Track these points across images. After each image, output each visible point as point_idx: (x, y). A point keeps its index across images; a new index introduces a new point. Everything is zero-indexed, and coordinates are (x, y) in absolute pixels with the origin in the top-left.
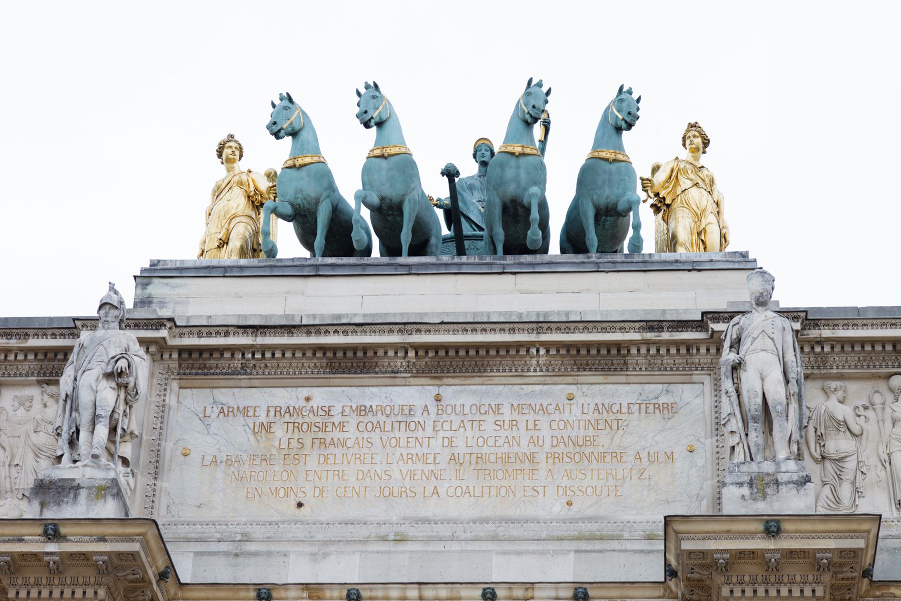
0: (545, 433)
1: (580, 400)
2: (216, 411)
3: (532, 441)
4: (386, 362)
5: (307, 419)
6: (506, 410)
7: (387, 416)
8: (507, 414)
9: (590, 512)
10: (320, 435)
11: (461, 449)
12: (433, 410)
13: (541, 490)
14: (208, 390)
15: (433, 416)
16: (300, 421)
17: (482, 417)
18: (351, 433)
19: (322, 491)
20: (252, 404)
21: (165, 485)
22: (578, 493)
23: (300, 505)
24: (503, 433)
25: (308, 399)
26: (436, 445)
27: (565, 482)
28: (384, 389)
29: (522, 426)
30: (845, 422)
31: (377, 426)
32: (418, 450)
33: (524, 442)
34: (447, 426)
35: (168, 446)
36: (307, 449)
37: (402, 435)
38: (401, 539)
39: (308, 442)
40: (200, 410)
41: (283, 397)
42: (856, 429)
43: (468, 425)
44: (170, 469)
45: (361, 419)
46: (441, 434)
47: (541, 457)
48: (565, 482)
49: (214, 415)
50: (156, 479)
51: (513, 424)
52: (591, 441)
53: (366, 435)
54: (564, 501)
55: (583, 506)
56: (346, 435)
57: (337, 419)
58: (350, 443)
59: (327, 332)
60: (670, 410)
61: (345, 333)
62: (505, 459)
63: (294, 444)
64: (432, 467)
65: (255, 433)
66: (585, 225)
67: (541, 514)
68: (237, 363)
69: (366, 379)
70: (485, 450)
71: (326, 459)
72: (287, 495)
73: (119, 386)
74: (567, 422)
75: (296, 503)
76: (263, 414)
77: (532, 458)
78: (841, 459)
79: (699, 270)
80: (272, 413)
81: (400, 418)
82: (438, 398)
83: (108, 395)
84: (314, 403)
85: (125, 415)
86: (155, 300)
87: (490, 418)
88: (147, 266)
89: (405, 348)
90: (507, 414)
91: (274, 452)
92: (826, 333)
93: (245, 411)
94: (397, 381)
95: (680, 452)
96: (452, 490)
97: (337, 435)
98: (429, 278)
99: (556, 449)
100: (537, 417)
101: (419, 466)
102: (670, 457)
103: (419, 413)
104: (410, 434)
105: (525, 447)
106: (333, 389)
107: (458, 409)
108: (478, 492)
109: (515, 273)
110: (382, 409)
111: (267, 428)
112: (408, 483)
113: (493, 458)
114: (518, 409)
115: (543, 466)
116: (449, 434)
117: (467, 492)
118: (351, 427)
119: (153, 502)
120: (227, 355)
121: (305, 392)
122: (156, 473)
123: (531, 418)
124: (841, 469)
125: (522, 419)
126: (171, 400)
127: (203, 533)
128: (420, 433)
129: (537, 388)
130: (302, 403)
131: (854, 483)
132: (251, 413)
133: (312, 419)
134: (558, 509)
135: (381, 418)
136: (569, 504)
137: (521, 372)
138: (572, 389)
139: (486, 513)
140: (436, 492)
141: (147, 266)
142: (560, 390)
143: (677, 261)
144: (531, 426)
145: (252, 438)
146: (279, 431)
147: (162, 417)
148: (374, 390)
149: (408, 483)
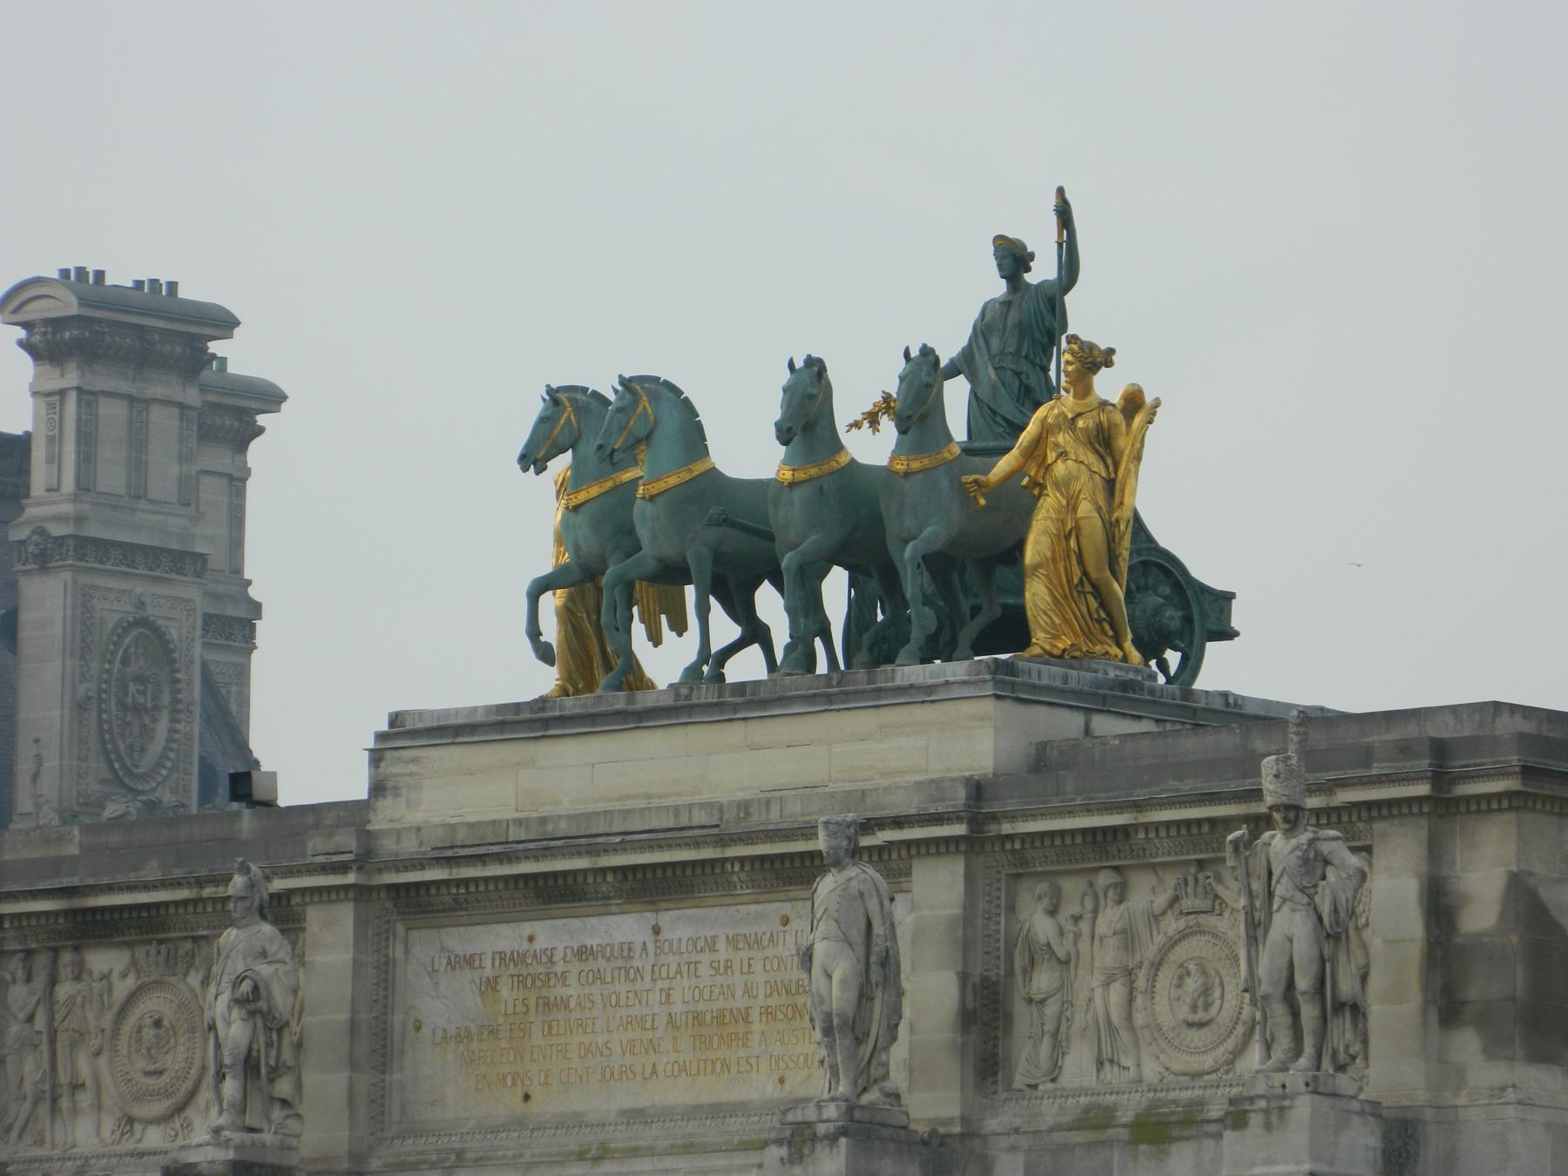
0: (759, 977)
2: (444, 961)
3: (748, 992)
5: (531, 970)
6: (721, 944)
7: (608, 959)
8: (723, 953)
10: (544, 992)
11: (678, 1008)
12: (651, 948)
13: (753, 1061)
14: (434, 932)
15: (651, 958)
16: (524, 972)
17: (699, 957)
18: (572, 990)
19: (547, 1077)
20: (474, 949)
21: (396, 1076)
22: (791, 1065)
23: (527, 1097)
24: (719, 980)
25: (531, 939)
26: (654, 998)
27: (777, 1049)
28: (604, 919)
29: (736, 967)
30: (1048, 944)
31: (598, 976)
33: (739, 992)
34: (664, 974)
35: (398, 1018)
36: (532, 1017)
37: (622, 987)
38: (603, 1154)
39: (532, 1003)
40: (428, 960)
41: (505, 937)
42: (1061, 953)
43: (684, 969)
44: (402, 1053)
45: (583, 966)
46: (659, 984)
47: (755, 1015)
48: (777, 1049)
49: (442, 969)
50: (384, 1072)
51: (728, 966)
53: (587, 990)
54: (776, 1076)
56: (570, 991)
57: (559, 968)
58: (573, 1003)
59: (518, 859)
61: (536, 859)
62: (720, 1019)
63: (520, 1008)
64: (650, 1034)
65: (482, 993)
66: (899, 565)
67: (755, 1096)
68: (448, 899)
70: (702, 1007)
71: (550, 1028)
72: (514, 1083)
73: (252, 1014)
74: (781, 960)
75: (520, 1094)
76: (488, 963)
77: (746, 1021)
78: (1042, 1002)
79: (933, 702)
80: (497, 963)
81: (619, 963)
82: (656, 930)
83: (236, 1032)
84: (540, 944)
85: (269, 1045)
86: (389, 785)
87: (706, 958)
88: (384, 727)
89: (603, 871)
90: (723, 953)
91: (501, 1021)
92: (1006, 828)
93: (470, 961)
94: (614, 909)
96: (669, 1067)
98: (659, 732)
99: (770, 1002)
100: (753, 954)
103: (637, 956)
104: (631, 987)
105: (740, 1002)
106: (555, 922)
107: (675, 945)
108: (694, 1071)
109: (744, 719)
110: (602, 948)
111: (492, 985)
112: (628, 1060)
113: (708, 1018)
114: (733, 942)
115: (757, 1027)
116: (665, 984)
117: (684, 1069)
118: (572, 980)
119: (383, 1105)
120: (433, 891)
121: (527, 928)
122: (384, 1064)
124: (1041, 1015)
126: (398, 952)
127: (422, 1153)
128: (639, 985)
129: (753, 908)
131: (1055, 1035)
132: (477, 964)
135: (602, 963)
136: (782, 1081)
138: (786, 908)
139: (706, 1098)
140: (654, 1072)
141: (384, 727)
143: (911, 686)
144: (745, 969)
145: (479, 1000)
146: (505, 991)
147: (386, 980)
148: (594, 920)
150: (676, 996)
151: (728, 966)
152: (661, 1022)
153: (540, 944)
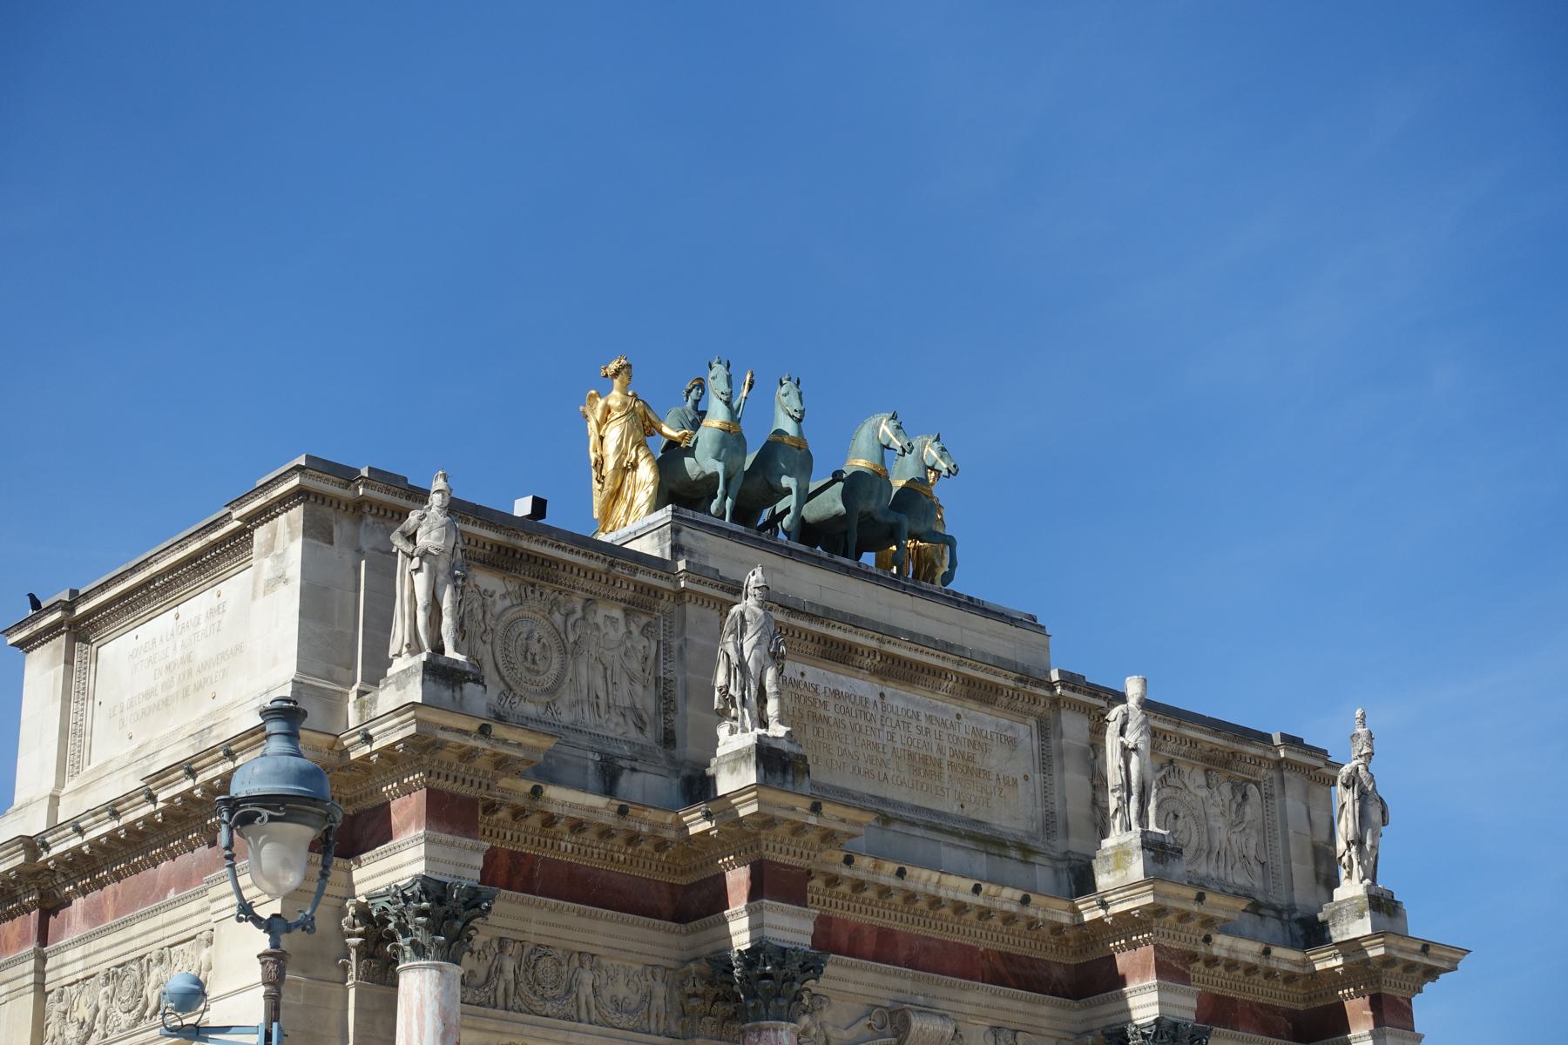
0: (946, 744)
1: (964, 721)
3: (940, 750)
4: (858, 658)
6: (922, 717)
9: (974, 816)
11: (898, 745)
26: (884, 735)
31: (847, 711)
32: (872, 739)
37: (862, 722)
47: (945, 765)
52: (971, 758)
55: (971, 812)
56: (828, 714)
57: (822, 698)
60: (1012, 743)
62: (924, 759)
69: (841, 667)
70: (913, 749)
77: (940, 765)
82: (882, 695)
87: (914, 723)
90: (924, 723)
95: (1021, 781)
97: (821, 711)
101: (874, 753)
102: (1015, 782)
105: (935, 755)
112: (869, 766)
114: (929, 718)
115: (946, 772)
118: (831, 707)
123: (936, 727)
125: (933, 728)
130: (799, 677)
133: (806, 693)
134: (955, 809)
137: (935, 689)
138: (959, 710)
142: (954, 707)
149: (869, 766)
150: (897, 738)
151: (928, 732)
152: (889, 750)
153: (808, 679)
